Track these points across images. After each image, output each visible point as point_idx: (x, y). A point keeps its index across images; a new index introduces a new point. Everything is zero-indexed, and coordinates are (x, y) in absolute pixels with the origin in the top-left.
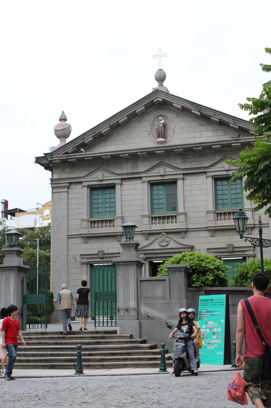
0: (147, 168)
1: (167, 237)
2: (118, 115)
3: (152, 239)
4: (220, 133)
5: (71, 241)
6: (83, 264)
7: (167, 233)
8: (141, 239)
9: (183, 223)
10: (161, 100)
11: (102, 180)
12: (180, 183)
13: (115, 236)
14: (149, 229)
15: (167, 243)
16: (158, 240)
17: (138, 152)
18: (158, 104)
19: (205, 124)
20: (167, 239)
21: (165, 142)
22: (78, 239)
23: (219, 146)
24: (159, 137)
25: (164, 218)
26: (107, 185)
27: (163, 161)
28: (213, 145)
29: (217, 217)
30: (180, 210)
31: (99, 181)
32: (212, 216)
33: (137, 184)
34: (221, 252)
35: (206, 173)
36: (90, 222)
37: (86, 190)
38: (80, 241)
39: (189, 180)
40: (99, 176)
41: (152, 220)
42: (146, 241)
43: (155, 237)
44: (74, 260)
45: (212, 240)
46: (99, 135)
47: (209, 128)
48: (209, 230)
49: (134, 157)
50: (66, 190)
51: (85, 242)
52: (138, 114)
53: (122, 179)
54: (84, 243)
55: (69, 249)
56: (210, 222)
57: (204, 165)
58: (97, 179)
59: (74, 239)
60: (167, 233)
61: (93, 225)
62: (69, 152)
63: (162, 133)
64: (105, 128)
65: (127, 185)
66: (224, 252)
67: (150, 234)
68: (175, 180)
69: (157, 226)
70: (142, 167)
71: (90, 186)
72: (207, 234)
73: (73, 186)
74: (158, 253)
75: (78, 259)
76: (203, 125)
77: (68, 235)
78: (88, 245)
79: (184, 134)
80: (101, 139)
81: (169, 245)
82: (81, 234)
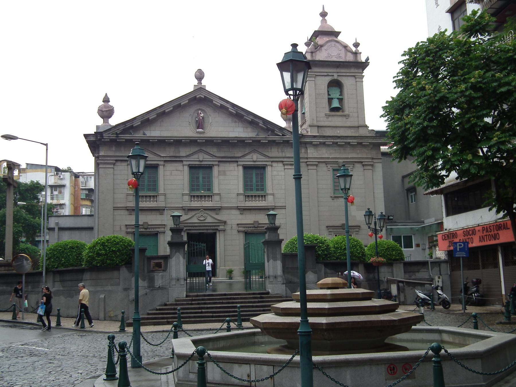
0: (188, 154)
1: (205, 213)
4: (249, 129)
5: (117, 212)
6: (128, 233)
7: (204, 209)
10: (203, 97)
12: (161, 168)
13: (158, 210)
17: (182, 140)
18: (199, 100)
19: (237, 120)
21: (204, 133)
22: (234, 211)
24: (198, 128)
25: (201, 196)
27: (202, 148)
30: (161, 191)
32: (242, 198)
33: (179, 166)
34: (249, 227)
35: (237, 162)
39: (224, 167)
43: (193, 213)
45: (243, 217)
47: (241, 124)
48: (239, 209)
49: (178, 143)
50: (112, 166)
53: (165, 161)
59: (119, 211)
63: (200, 124)
65: (170, 167)
67: (189, 210)
70: (183, 152)
72: (237, 212)
73: (118, 164)
76: (235, 122)
79: (219, 128)
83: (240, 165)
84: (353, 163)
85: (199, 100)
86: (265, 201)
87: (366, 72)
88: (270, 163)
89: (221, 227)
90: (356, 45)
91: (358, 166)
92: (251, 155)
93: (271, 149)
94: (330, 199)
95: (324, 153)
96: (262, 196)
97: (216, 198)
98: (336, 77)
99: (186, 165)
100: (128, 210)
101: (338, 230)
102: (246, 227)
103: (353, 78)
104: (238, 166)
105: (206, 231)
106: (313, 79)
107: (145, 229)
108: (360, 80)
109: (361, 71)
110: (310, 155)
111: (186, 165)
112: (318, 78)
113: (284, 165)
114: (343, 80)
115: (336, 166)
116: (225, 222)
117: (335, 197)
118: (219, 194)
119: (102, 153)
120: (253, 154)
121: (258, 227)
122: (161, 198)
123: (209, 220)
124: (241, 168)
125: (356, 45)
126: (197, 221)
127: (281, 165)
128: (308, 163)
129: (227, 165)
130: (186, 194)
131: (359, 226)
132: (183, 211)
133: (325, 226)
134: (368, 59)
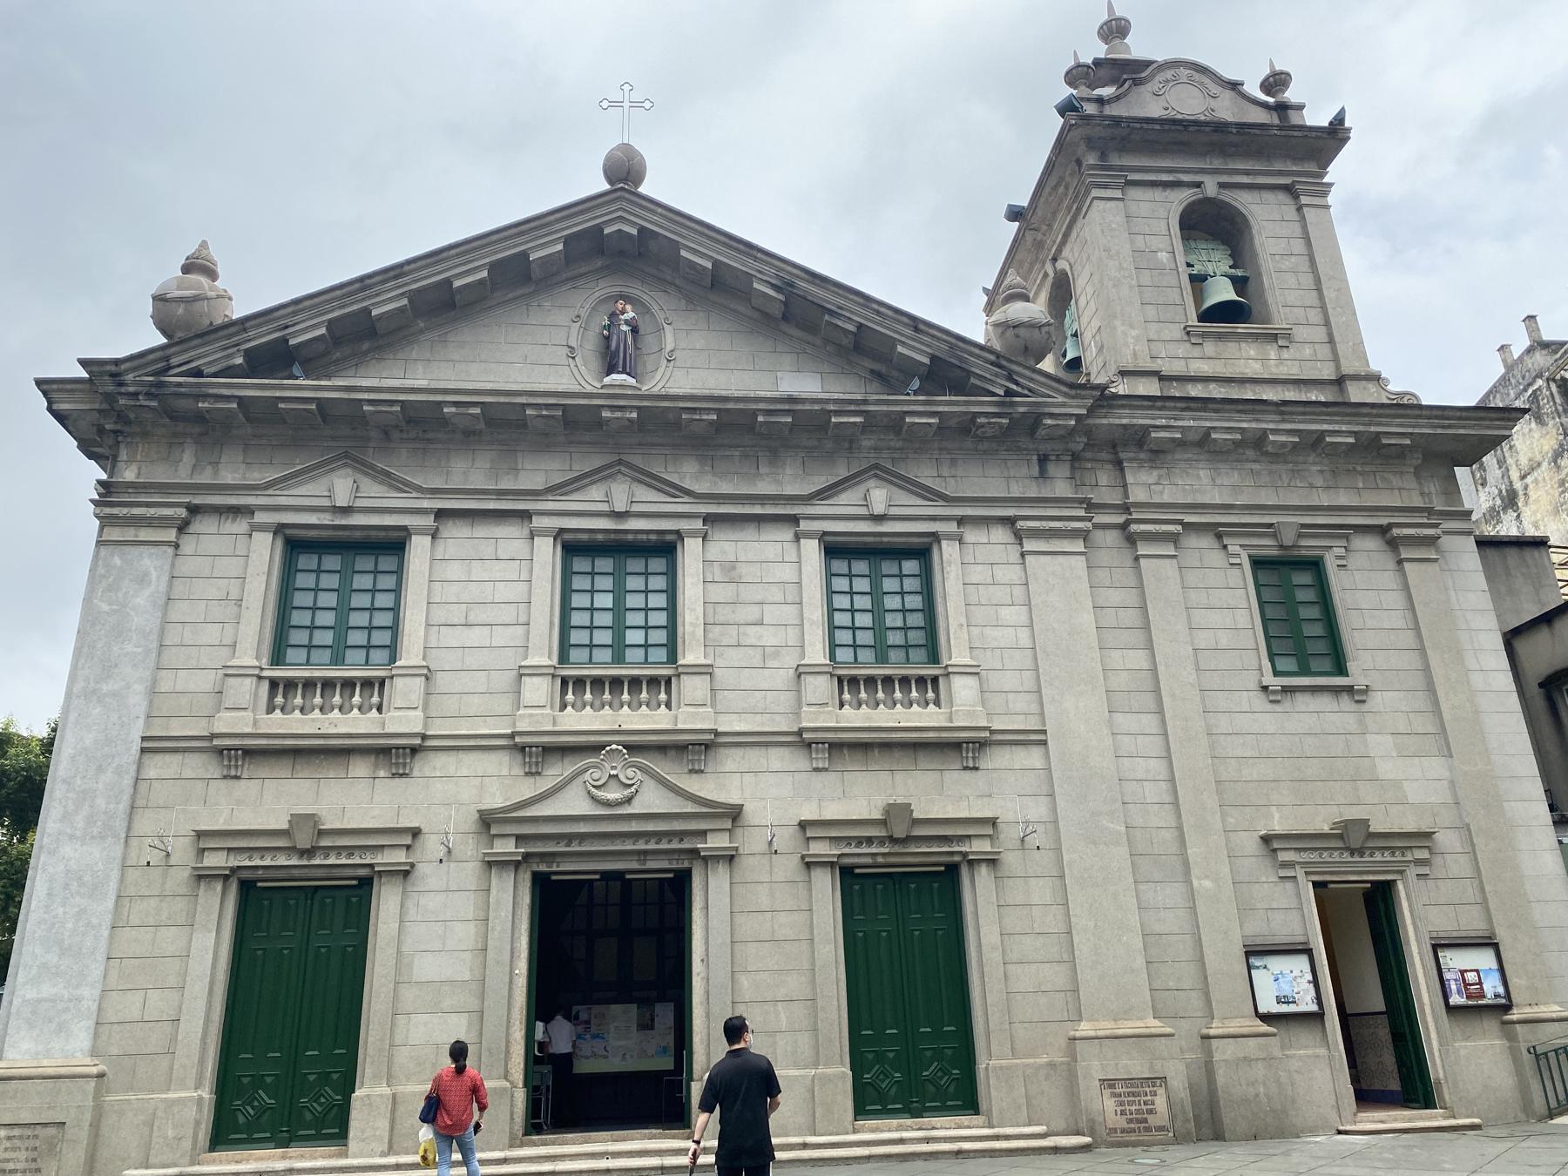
2: (453, 252)
3: (555, 772)
5: (158, 767)
7: (632, 748)
8: (505, 772)
9: (701, 710)
11: (347, 510)
14: (549, 728)
15: (627, 792)
16: (587, 776)
20: (630, 772)
23: (858, 419)
24: (611, 370)
26: (365, 533)
27: (624, 457)
28: (838, 413)
29: (841, 692)
31: (336, 510)
32: (820, 687)
33: (509, 538)
34: (860, 841)
36: (265, 685)
37: (264, 552)
38: (198, 766)
39: (726, 545)
40: (338, 493)
41: (564, 692)
42: (531, 780)
44: (156, 857)
46: (362, 321)
49: (505, 425)
51: (233, 773)
52: (536, 273)
53: (440, 514)
54: (225, 777)
55: (140, 802)
56: (813, 709)
57: (789, 490)
58: (326, 503)
60: (632, 748)
61: (279, 700)
64: (391, 300)
66: (869, 840)
69: (584, 719)
70: (535, 473)
71: (288, 532)
73: (204, 525)
74: (582, 837)
75: (182, 852)
77: (144, 739)
78: (246, 788)
80: (366, 346)
81: (635, 801)
82: (213, 736)
83: (809, 535)
85: (620, 246)
86: (937, 703)
87: (1340, 171)
88: (952, 527)
89: (717, 842)
90: (1276, 82)
91: (1371, 543)
92: (861, 489)
93: (953, 462)
94: (1260, 701)
95: (1202, 485)
96: (921, 681)
97: (692, 688)
98: (1211, 189)
102: (848, 840)
103: (1282, 197)
104: (797, 538)
105: (635, 865)
106: (1118, 194)
107: (303, 853)
109: (1312, 167)
110: (1138, 495)
111: (543, 533)
112: (1134, 193)
113: (1019, 537)
114: (1246, 202)
115: (1267, 547)
116: (734, 814)
117: (1286, 690)
118: (705, 670)
119: (129, 475)
120: (872, 483)
122: (405, 691)
123: (652, 800)
124: (812, 549)
125: (1276, 82)
126: (583, 807)
127: (1000, 534)
128: (1134, 527)
129: (749, 533)
130: (536, 672)
131: (1428, 835)
132: (519, 757)
133: (1256, 836)
134: (1339, 120)
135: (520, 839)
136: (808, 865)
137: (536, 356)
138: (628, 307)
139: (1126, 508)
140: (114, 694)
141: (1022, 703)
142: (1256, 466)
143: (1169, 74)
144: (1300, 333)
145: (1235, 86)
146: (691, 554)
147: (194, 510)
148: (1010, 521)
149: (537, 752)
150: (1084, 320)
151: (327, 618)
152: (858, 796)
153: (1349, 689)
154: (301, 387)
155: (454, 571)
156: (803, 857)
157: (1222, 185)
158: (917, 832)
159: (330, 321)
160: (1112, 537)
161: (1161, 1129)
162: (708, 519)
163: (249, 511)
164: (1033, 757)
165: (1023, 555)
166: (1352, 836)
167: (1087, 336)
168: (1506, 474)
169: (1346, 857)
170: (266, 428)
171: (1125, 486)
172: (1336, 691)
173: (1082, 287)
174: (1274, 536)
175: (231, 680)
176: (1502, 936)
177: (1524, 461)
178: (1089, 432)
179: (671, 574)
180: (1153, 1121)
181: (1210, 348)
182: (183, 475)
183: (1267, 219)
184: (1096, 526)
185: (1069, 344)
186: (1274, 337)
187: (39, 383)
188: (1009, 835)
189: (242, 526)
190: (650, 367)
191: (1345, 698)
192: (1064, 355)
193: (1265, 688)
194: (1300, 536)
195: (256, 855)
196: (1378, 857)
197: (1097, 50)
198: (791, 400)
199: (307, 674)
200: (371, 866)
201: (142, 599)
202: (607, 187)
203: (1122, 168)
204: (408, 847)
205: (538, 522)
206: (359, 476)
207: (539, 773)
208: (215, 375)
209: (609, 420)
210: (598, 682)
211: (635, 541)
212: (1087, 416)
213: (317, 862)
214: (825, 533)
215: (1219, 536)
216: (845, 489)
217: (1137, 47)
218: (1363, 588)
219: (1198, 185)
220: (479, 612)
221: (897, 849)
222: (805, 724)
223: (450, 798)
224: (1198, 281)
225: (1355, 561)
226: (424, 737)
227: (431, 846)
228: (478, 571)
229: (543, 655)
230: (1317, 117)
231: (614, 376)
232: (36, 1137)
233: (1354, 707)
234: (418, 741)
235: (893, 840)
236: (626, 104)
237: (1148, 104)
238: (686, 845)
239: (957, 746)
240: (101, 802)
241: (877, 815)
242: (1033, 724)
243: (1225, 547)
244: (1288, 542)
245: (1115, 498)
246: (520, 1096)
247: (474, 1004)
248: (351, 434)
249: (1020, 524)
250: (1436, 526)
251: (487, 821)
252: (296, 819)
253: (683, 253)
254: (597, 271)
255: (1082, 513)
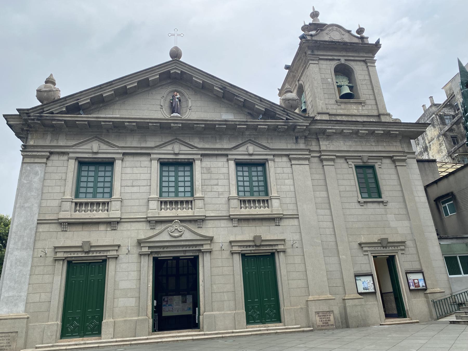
0: (158, 144)
2: (127, 78)
3: (160, 228)
5: (42, 228)
7: (182, 221)
9: (201, 210)
10: (179, 72)
14: (157, 216)
15: (180, 234)
16: (169, 229)
20: (181, 228)
23: (245, 127)
28: (239, 125)
29: (241, 204)
32: (235, 203)
33: (144, 161)
34: (247, 246)
35: (227, 155)
36: (74, 204)
37: (73, 165)
38: (54, 228)
39: (207, 162)
40: (94, 148)
42: (152, 230)
44: (43, 254)
46: (100, 98)
49: (143, 128)
51: (65, 230)
52: (151, 84)
53: (124, 154)
54: (62, 231)
55: (37, 239)
56: (233, 209)
57: (225, 147)
58: (90, 151)
60: (182, 221)
61: (78, 208)
62: (55, 112)
64: (109, 92)
68: (191, 161)
69: (167, 213)
71: (80, 159)
73: (54, 157)
74: (167, 247)
75: (50, 253)
77: (38, 220)
80: (101, 105)
81: (183, 236)
82: (59, 219)
84: (380, 158)
85: (175, 76)
86: (268, 207)
88: (271, 157)
89: (206, 247)
91: (388, 161)
92: (246, 146)
94: (358, 206)
96: (263, 201)
97: (198, 203)
98: (343, 61)
99: (154, 159)
100: (61, 224)
101: (376, 249)
102: (243, 246)
103: (362, 63)
104: (228, 160)
105: (182, 255)
108: (372, 65)
109: (371, 55)
110: (323, 148)
111: (154, 159)
112: (321, 62)
113: (290, 160)
114: (352, 65)
115: (359, 162)
116: (211, 239)
118: (202, 198)
119: (31, 143)
120: (249, 145)
121: (261, 246)
122: (115, 205)
123: (187, 235)
124: (232, 164)
125: (360, 31)
126: (168, 238)
127: (285, 159)
128: (322, 157)
129: (214, 159)
130: (153, 199)
131: (404, 242)
132: (149, 225)
133: (357, 243)
134: (378, 42)
135: (149, 247)
136: (232, 253)
137: (152, 108)
138: (178, 94)
139: (320, 152)
140: (29, 207)
141: (291, 207)
142: (356, 140)
143: (331, 28)
144: (368, 102)
145: (349, 32)
146: (197, 166)
147: (51, 153)
148: (288, 155)
149: (154, 222)
150: (307, 98)
151: (91, 185)
152: (246, 233)
153: (382, 202)
154: (83, 117)
155: (128, 170)
156: (231, 251)
157: (346, 60)
158: (263, 243)
159: (91, 98)
160: (316, 160)
161: (332, 325)
162: (202, 155)
163: (67, 153)
164: (295, 222)
165: (291, 165)
166: (384, 243)
167: (308, 102)
168: (425, 142)
169: (382, 249)
170: (74, 129)
171: (320, 145)
172: (379, 202)
173: (307, 89)
174: (361, 159)
175: (64, 202)
176: (424, 270)
177: (429, 138)
178: (310, 130)
179: (192, 171)
180: (330, 323)
181: (343, 106)
182: (47, 143)
183: (358, 69)
184: (312, 157)
185: (303, 105)
186: (361, 103)
187: (4, 116)
188: (288, 244)
189: (65, 158)
190: (184, 111)
191: (381, 204)
192: (302, 108)
193: (359, 202)
194: (368, 159)
195: (72, 253)
196: (390, 248)
197: (309, 20)
198: (226, 121)
199: (86, 201)
200: (106, 256)
201: (36, 179)
202: (171, 59)
203: (318, 55)
204: (117, 250)
205: (153, 156)
206: (100, 143)
207: (154, 229)
208: (57, 114)
209: (173, 126)
210: (171, 202)
211: (181, 162)
212: (309, 126)
213: (90, 255)
214: (236, 159)
215: (346, 159)
216: (241, 146)
217: (322, 19)
218: (386, 174)
219: (339, 60)
220: (136, 182)
221: (257, 248)
222: (231, 214)
223: (128, 236)
224: (339, 87)
225: (383, 166)
226: (121, 219)
227: (123, 250)
228: (135, 170)
229: (155, 195)
230: (372, 41)
231: (174, 114)
232: (9, 336)
233: (384, 207)
234: (119, 220)
235: (256, 246)
236: (176, 35)
237: (325, 37)
238: (197, 248)
239: (273, 219)
240: (26, 239)
241: (251, 239)
242: (295, 213)
243: (348, 162)
244: (365, 161)
245: (317, 149)
246: (151, 321)
247: (137, 295)
248: (98, 131)
249: (291, 156)
250: (406, 156)
251: (140, 243)
252: (84, 243)
253: (194, 78)
254: (170, 83)
255: (308, 153)
